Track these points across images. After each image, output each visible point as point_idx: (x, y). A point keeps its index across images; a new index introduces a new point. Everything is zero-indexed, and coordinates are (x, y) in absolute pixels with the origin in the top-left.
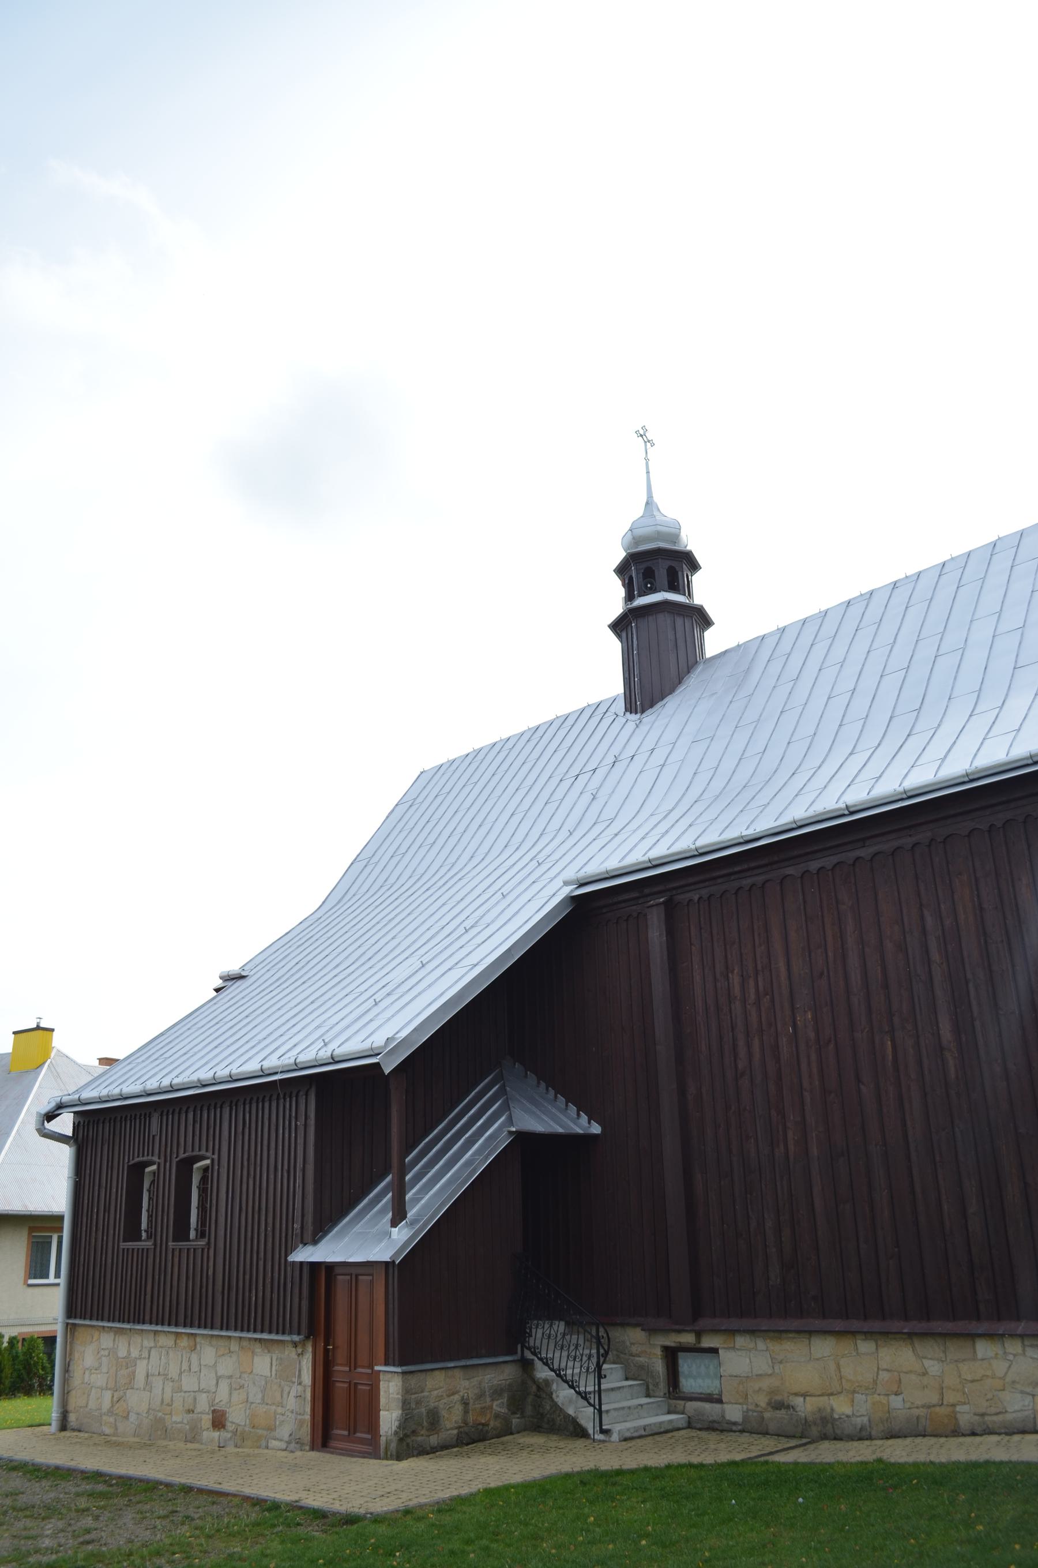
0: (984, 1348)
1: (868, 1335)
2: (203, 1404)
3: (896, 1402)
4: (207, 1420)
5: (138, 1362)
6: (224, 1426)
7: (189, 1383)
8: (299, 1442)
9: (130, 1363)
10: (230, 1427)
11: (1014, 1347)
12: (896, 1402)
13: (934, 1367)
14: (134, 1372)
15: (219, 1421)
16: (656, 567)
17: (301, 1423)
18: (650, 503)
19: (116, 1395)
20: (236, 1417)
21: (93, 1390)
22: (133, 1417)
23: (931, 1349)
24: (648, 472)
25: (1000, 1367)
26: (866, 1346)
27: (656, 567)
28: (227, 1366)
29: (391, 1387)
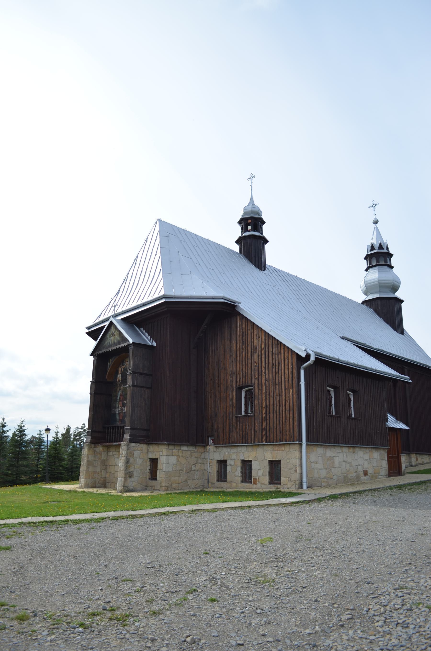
2: (360, 469)
4: (362, 474)
5: (335, 458)
6: (367, 475)
7: (354, 463)
8: (386, 476)
9: (331, 458)
10: (369, 474)
14: (334, 462)
15: (365, 473)
16: (252, 222)
20: (370, 471)
22: (335, 478)
24: (252, 190)
27: (252, 222)
28: (367, 457)
29: (404, 458)
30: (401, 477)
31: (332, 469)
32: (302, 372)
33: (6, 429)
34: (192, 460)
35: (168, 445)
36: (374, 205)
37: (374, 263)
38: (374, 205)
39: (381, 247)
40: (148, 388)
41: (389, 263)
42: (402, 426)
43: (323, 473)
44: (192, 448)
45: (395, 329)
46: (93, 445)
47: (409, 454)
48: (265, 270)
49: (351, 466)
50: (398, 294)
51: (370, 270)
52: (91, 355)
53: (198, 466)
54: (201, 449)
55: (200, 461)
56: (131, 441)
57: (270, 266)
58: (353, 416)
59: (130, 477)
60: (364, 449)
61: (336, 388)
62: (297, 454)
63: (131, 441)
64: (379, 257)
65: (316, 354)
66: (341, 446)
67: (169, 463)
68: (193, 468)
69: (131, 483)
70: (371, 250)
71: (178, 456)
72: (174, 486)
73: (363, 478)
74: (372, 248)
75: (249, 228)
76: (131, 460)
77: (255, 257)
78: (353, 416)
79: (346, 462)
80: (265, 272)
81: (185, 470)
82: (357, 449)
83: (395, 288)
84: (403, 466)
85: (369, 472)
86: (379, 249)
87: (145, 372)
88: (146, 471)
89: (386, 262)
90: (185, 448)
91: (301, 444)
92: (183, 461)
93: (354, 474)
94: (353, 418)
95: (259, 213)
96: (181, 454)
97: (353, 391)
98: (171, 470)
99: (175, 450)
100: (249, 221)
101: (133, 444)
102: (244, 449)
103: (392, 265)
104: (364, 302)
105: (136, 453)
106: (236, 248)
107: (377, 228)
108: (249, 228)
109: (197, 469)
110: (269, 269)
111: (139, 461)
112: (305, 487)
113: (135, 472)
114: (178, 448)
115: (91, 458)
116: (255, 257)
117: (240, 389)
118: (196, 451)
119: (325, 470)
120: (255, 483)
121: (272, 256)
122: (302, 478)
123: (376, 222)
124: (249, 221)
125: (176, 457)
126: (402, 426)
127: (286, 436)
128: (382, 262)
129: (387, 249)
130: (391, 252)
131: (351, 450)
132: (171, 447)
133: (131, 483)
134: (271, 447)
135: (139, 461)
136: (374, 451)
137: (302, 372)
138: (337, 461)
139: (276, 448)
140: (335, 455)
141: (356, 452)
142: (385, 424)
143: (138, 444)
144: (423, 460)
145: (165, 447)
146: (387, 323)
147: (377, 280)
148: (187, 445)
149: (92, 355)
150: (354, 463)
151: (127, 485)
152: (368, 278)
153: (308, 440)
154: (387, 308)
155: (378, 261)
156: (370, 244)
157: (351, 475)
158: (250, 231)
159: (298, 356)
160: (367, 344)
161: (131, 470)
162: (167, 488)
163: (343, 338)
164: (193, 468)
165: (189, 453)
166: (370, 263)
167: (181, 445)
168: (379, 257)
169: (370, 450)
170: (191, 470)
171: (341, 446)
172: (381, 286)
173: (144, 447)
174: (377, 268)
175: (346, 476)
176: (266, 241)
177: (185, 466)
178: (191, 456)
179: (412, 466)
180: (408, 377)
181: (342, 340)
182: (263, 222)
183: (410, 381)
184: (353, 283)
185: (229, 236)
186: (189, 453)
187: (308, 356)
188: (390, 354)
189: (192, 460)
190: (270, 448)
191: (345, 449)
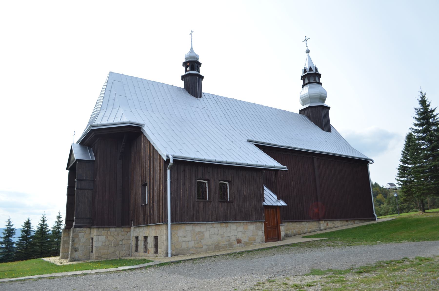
0: (303, 223)
1: (291, 222)
2: (233, 239)
3: (294, 231)
6: (241, 242)
11: (306, 223)
12: (294, 231)
13: (298, 226)
14: (204, 235)
16: (192, 64)
17: (263, 238)
18: (192, 49)
19: (196, 242)
21: (184, 243)
22: (204, 247)
23: (298, 223)
25: (305, 225)
26: (291, 224)
27: (192, 64)
29: (282, 228)
30: (280, 241)
31: (202, 241)
32: (169, 172)
33: (61, 220)
34: (120, 238)
35: (98, 228)
36: (306, 40)
37: (307, 82)
38: (306, 40)
39: (311, 69)
40: (90, 189)
41: (317, 81)
42: (282, 203)
43: (192, 244)
44: (118, 229)
45: (322, 128)
46: (67, 230)
47: (319, 221)
48: (201, 96)
49: (223, 237)
50: (327, 103)
51: (304, 87)
52: (67, 169)
53: (125, 242)
54: (127, 230)
55: (126, 238)
56: (76, 227)
57: (208, 94)
58: (229, 200)
59: (76, 251)
60: (239, 224)
61: (209, 181)
62: (164, 231)
63: (76, 227)
64: (311, 77)
65: (174, 157)
66: (212, 223)
67: (99, 241)
68: (120, 243)
69: (76, 255)
70: (305, 73)
71: (107, 236)
72: (103, 256)
73: (236, 245)
74: (305, 71)
75: (188, 69)
76: (77, 240)
77: (192, 89)
78: (229, 200)
79: (217, 234)
80: (201, 99)
81: (113, 245)
82: (229, 224)
83: (323, 99)
84: (283, 234)
85: (242, 240)
86: (309, 71)
87: (88, 179)
88: (89, 247)
89: (315, 80)
90: (113, 229)
91: (167, 224)
92: (110, 238)
93: (227, 243)
94: (229, 202)
95: (197, 57)
96: (109, 234)
97: (229, 182)
98: (101, 245)
99: (104, 231)
100: (188, 64)
101: (77, 229)
102: (144, 229)
103: (321, 82)
104: (301, 111)
105: (81, 235)
106: (181, 84)
107: (309, 56)
108: (188, 69)
109: (124, 243)
110: (207, 96)
111: (83, 240)
112: (169, 255)
113: (80, 248)
114: (107, 229)
115: (65, 239)
116: (192, 89)
117: (145, 185)
118: (123, 231)
119: (194, 242)
120: (148, 253)
121: (206, 87)
122: (167, 249)
123: (308, 52)
124: (188, 64)
125: (105, 236)
126: (282, 203)
127: (158, 219)
128: (312, 81)
129: (316, 70)
130: (320, 72)
131: (224, 225)
132: (100, 230)
133: (76, 255)
134: (154, 226)
135: (83, 240)
136: (249, 224)
137: (169, 172)
138: (207, 235)
139: (157, 227)
140: (205, 230)
141: (229, 226)
142: (261, 204)
143: (82, 228)
144: (334, 225)
145: (95, 230)
146: (316, 124)
147: (308, 94)
148: (115, 227)
149: (67, 169)
150: (225, 235)
151: (73, 256)
152: (302, 94)
153: (172, 221)
154: (317, 114)
155: (309, 80)
156: (304, 69)
157: (222, 244)
158: (189, 71)
159: (164, 160)
160: (272, 143)
161: (76, 246)
162: (97, 258)
163: (249, 141)
164: (120, 243)
165: (116, 233)
166: (304, 82)
167: (109, 228)
168: (311, 77)
169: (245, 223)
170: (118, 244)
171: (212, 223)
172: (311, 98)
173: (87, 230)
174: (308, 85)
175: (217, 245)
176: (202, 77)
177: (113, 242)
178: (118, 235)
179: (321, 230)
180: (286, 167)
181: (249, 143)
182: (200, 64)
183: (287, 169)
184: (292, 98)
185: (175, 77)
186: (116, 233)
187: (168, 160)
188: (298, 148)
189: (120, 238)
190: (154, 228)
191: (215, 225)
